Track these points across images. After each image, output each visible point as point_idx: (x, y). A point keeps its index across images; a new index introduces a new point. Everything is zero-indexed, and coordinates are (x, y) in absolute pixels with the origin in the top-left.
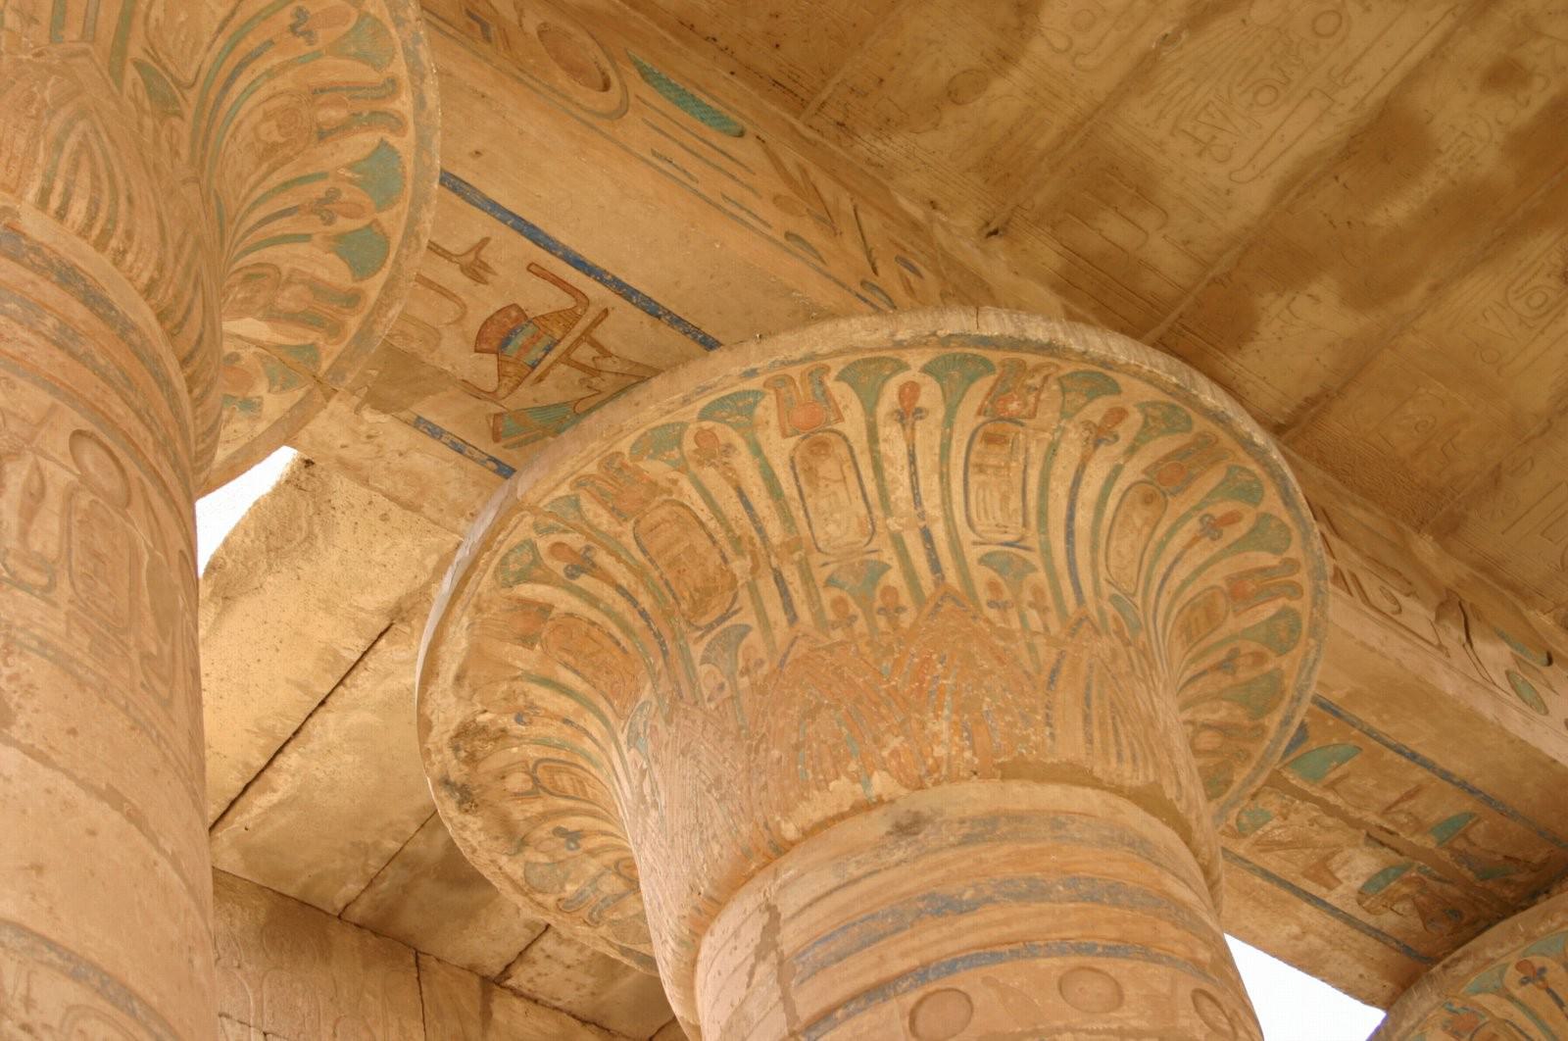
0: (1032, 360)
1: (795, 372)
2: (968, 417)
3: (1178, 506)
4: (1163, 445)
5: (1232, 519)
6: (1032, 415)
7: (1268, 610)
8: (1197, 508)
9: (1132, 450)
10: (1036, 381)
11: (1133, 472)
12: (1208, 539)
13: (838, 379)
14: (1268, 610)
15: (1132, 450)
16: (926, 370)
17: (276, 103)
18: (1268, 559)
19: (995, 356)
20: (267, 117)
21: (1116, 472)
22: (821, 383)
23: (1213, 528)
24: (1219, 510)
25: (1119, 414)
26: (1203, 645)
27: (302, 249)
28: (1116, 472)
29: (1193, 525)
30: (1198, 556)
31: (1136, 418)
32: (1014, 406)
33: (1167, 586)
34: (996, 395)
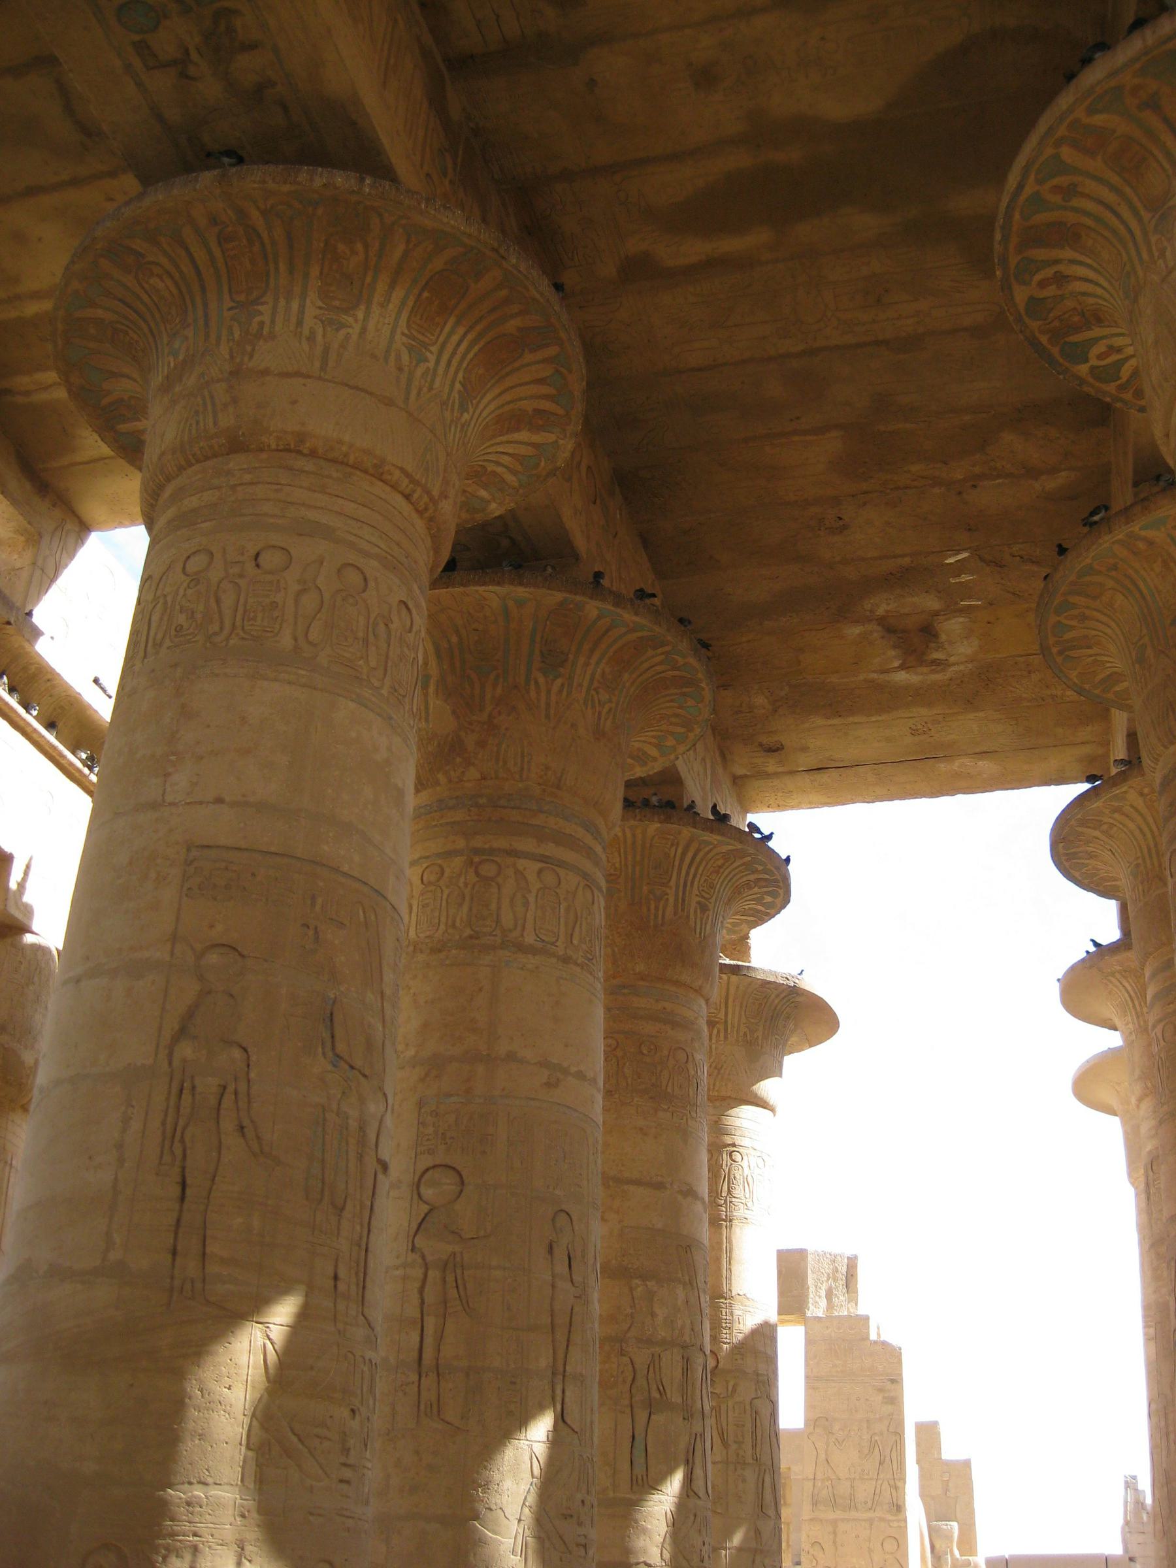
0: (1044, 339)
1: (1128, 396)
2: (1096, 332)
4: (1040, 254)
5: (1056, 189)
6: (1075, 309)
9: (1056, 262)
10: (1057, 323)
13: (1119, 378)
15: (1056, 262)
16: (1086, 360)
18: (1066, 152)
19: (1055, 351)
20: (1152, 569)
21: (1072, 262)
22: (1128, 381)
23: (1070, 191)
24: (1056, 199)
25: (1043, 284)
28: (1072, 262)
29: (1075, 203)
31: (1038, 277)
32: (1076, 319)
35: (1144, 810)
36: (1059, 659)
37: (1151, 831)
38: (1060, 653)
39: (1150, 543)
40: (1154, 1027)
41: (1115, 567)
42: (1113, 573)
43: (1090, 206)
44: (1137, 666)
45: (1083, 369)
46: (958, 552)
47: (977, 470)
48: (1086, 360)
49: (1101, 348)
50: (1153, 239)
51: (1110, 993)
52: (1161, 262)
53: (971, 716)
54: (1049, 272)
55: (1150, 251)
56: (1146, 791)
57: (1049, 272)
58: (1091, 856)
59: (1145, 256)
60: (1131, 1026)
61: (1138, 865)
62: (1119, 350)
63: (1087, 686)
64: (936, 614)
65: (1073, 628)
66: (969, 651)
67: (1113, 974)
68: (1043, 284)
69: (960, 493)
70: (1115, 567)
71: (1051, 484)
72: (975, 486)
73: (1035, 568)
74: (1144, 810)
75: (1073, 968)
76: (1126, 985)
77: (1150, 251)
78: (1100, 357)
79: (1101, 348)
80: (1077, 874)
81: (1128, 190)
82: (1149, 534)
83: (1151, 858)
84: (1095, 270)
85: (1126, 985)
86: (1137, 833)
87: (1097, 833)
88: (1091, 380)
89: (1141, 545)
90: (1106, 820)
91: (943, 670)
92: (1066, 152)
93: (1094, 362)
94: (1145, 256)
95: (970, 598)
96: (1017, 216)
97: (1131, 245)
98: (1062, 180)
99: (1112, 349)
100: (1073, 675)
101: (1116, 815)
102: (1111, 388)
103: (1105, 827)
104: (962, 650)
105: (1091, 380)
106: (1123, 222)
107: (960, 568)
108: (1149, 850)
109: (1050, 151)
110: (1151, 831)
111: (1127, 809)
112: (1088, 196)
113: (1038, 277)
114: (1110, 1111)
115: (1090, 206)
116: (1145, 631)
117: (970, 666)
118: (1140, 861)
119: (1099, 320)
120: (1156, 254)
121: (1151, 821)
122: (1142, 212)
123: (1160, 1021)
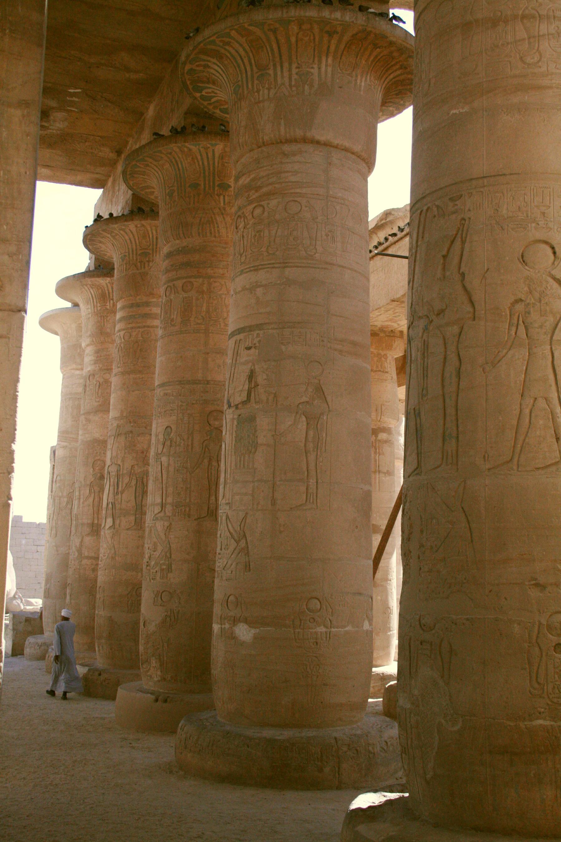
0: (188, 83)
1: (211, 107)
2: (211, 86)
3: (223, 51)
4: (203, 57)
7: (251, 28)
8: (222, 47)
9: (209, 61)
11: (215, 61)
12: (231, 44)
14: (251, 28)
15: (209, 61)
17: (184, 158)
18: (233, 33)
19: (191, 87)
20: (187, 160)
21: (214, 63)
25: (197, 66)
26: (264, 40)
27: (216, 150)
28: (214, 63)
29: (227, 47)
30: (236, 46)
31: (197, 63)
33: (243, 58)
34: (203, 82)
35: (135, 233)
36: (128, 176)
37: (136, 243)
38: (130, 174)
39: (190, 150)
40: (119, 331)
41: (171, 153)
42: (169, 155)
43: (233, 51)
44: (168, 197)
45: (198, 95)
46: (76, 88)
47: (103, 62)
48: (201, 92)
49: (210, 90)
50: (256, 82)
51: (82, 292)
52: (256, 94)
53: (48, 150)
54: (202, 63)
55: (253, 86)
56: (139, 226)
57: (202, 63)
58: (101, 242)
59: (250, 86)
60: (90, 310)
61: (125, 256)
62: (216, 93)
63: (135, 188)
64: (53, 108)
65: (139, 167)
66: (61, 126)
67: (86, 285)
68: (197, 66)
69: (90, 67)
70: (171, 153)
71: (133, 76)
72: (98, 67)
73: (109, 104)
74: (135, 233)
75: (68, 278)
76: (92, 291)
77: (253, 86)
78: (206, 93)
79: (210, 90)
80: (90, 247)
81: (251, 54)
82: (191, 147)
83: (133, 254)
84: (223, 71)
85: (92, 291)
86: (128, 241)
87: (109, 236)
88: (199, 99)
89: (186, 149)
90: (115, 232)
91: (45, 130)
92: (233, 33)
93: (203, 93)
94: (250, 86)
95: (73, 107)
96: (202, 45)
97: (244, 75)
98: (227, 40)
99: (213, 92)
100: (131, 183)
101: (121, 232)
102: (205, 103)
103: (113, 234)
104: (58, 125)
105: (199, 99)
106: (243, 61)
107: (74, 95)
108: (133, 251)
109: (227, 31)
110: (136, 243)
111: (127, 230)
112: (234, 48)
113: (197, 63)
114: (56, 334)
115: (233, 51)
116: (175, 184)
117: (59, 132)
118: (127, 254)
119: (214, 83)
120: (255, 89)
121: (137, 238)
122: (254, 68)
123: (124, 330)
